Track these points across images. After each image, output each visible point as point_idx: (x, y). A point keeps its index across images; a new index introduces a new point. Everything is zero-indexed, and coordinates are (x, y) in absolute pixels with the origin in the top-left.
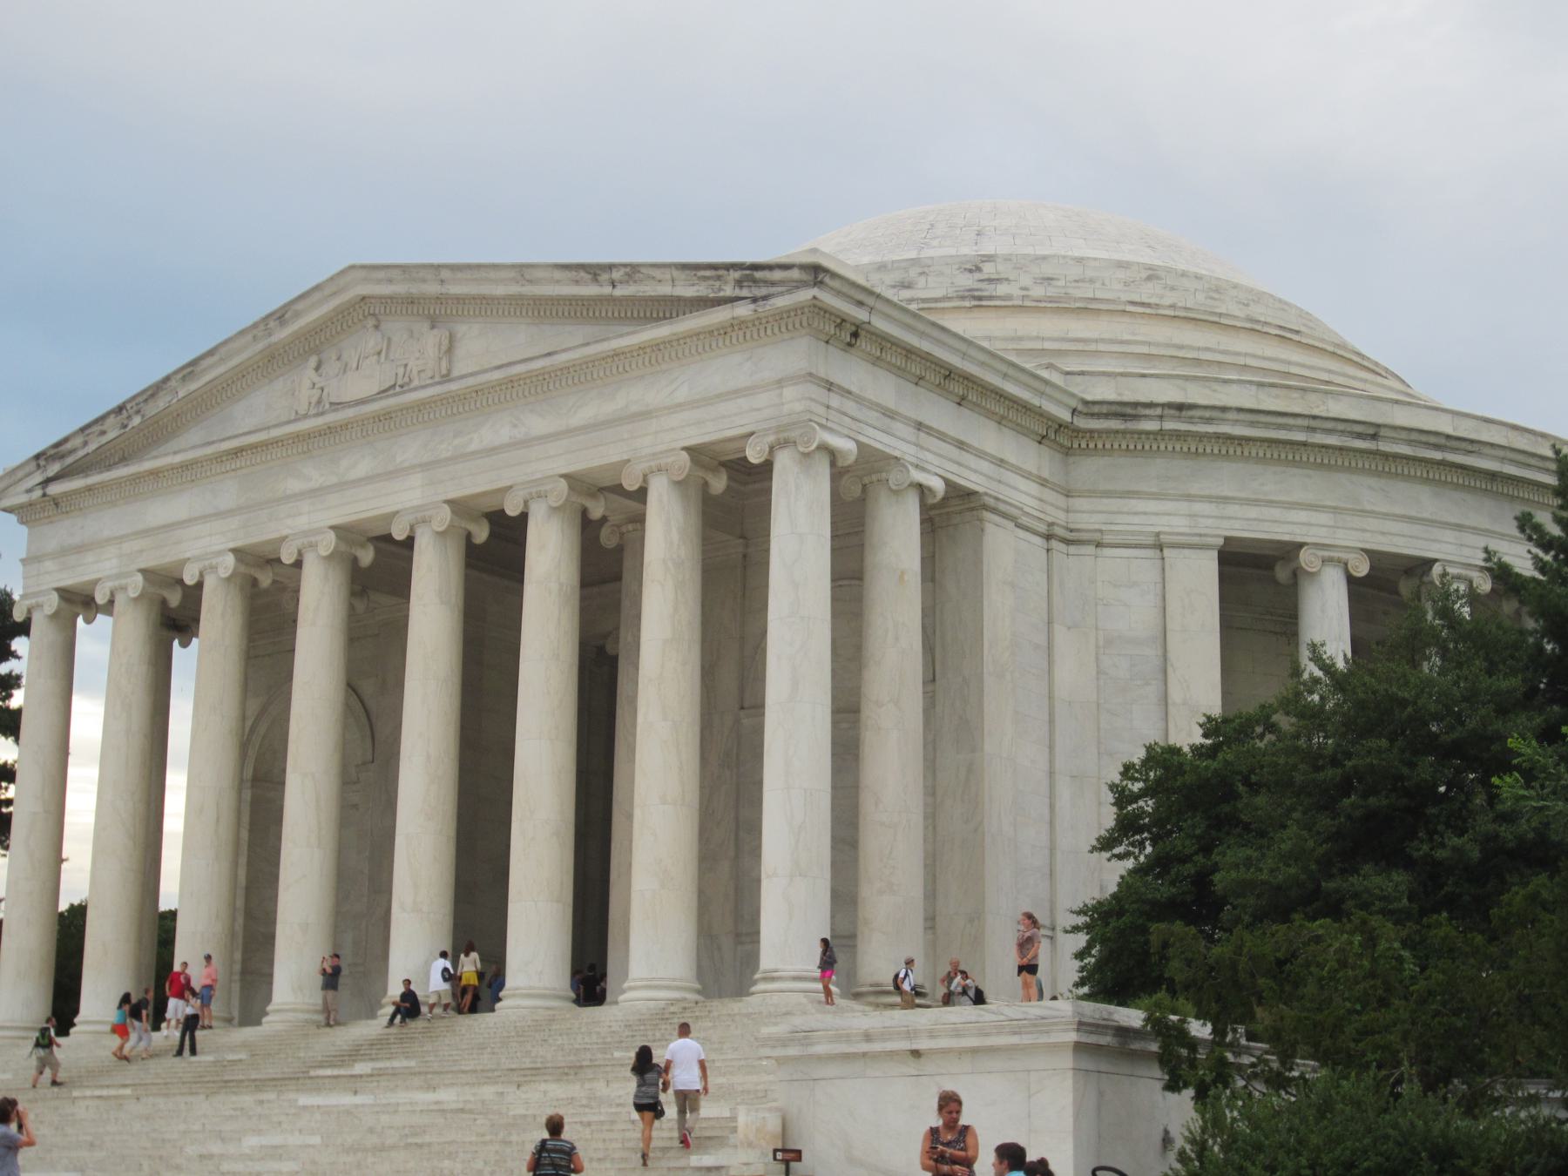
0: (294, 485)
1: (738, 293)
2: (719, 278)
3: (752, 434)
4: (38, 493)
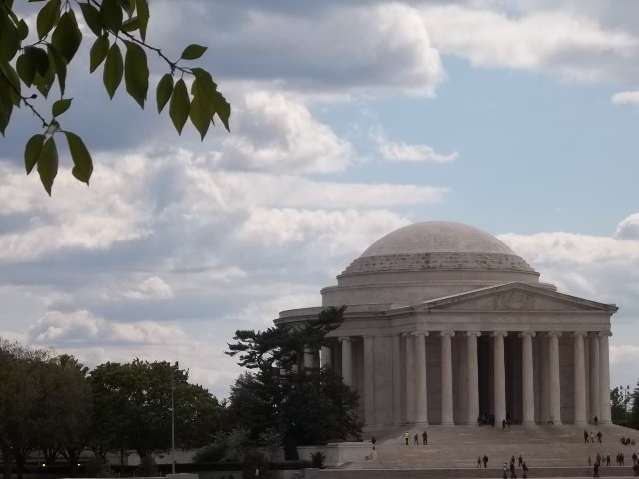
0: (495, 321)
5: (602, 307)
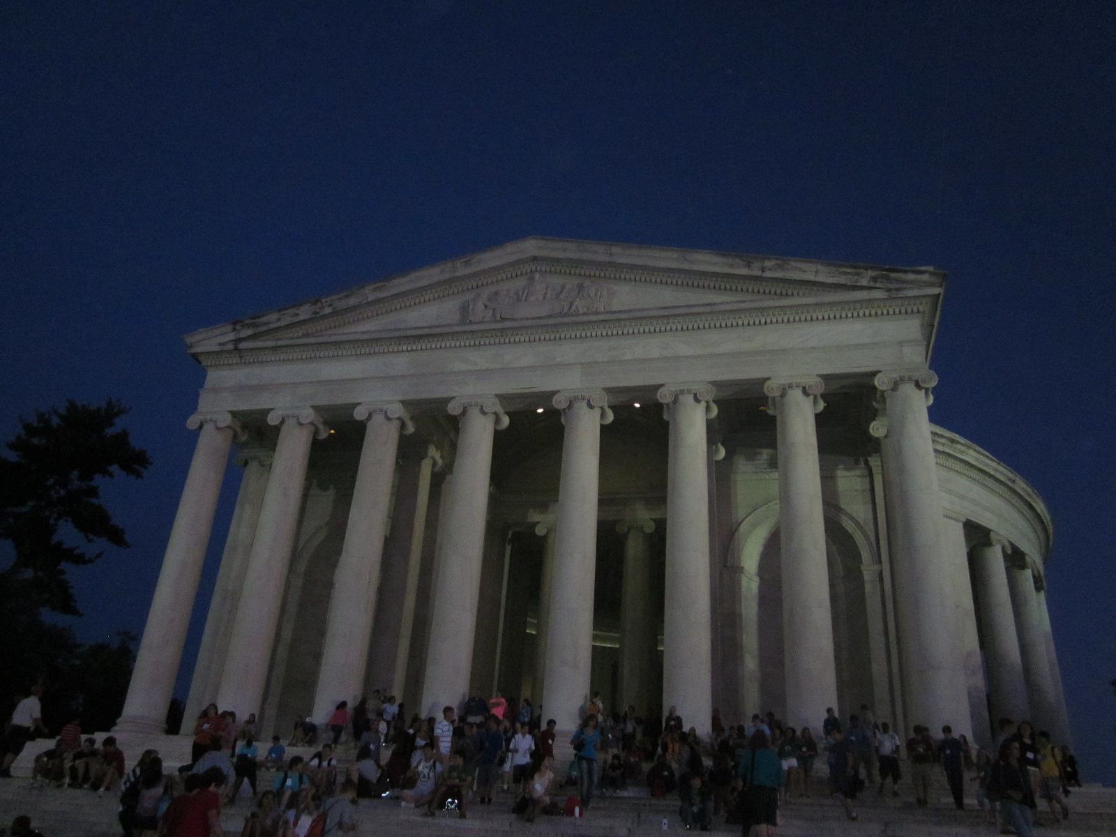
0: (460, 366)
1: (872, 284)
2: (858, 274)
3: (880, 372)
4: (231, 347)
5: (874, 279)
